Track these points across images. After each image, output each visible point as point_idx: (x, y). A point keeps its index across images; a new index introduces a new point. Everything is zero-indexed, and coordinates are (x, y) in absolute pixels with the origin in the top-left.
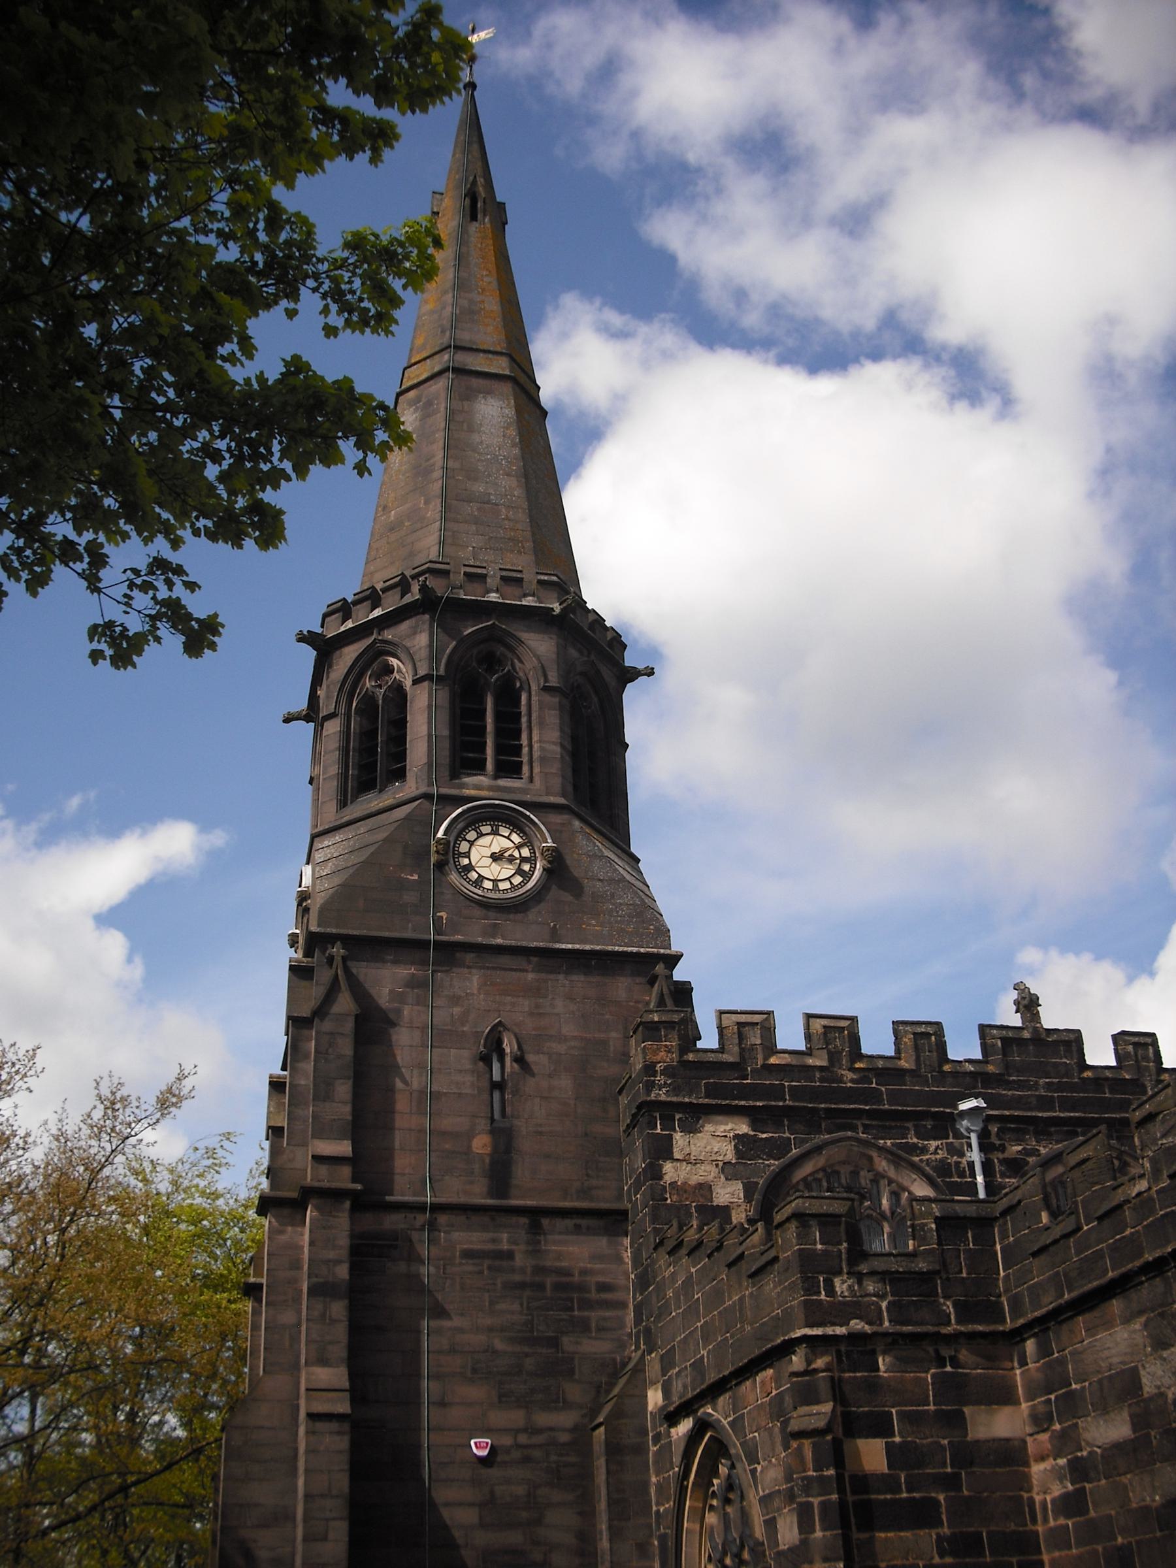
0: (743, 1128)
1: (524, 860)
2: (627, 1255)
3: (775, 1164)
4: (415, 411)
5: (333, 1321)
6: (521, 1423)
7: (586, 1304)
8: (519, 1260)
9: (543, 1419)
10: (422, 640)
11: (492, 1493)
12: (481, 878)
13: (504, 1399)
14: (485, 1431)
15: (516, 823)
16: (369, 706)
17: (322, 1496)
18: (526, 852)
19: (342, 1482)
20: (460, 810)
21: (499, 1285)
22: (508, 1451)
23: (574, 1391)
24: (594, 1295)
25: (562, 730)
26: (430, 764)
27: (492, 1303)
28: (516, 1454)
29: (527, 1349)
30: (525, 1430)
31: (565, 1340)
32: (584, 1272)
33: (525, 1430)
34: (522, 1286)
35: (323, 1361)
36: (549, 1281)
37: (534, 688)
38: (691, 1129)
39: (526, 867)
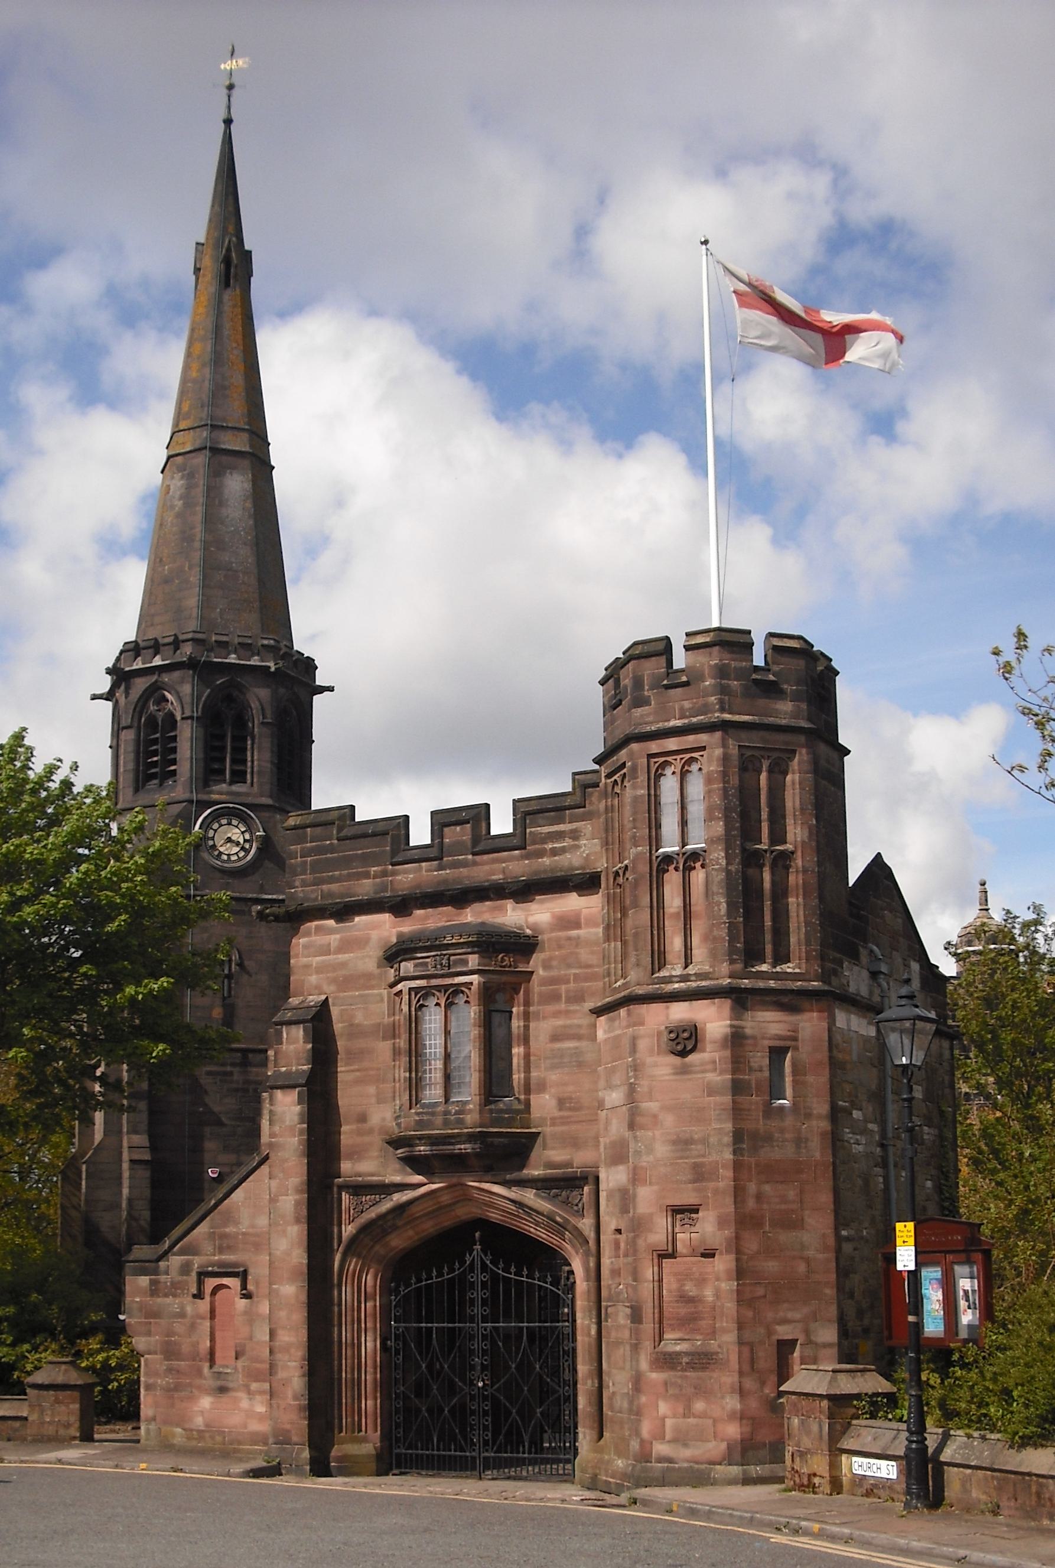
1: (245, 841)
4: (182, 478)
8: (235, 1077)
10: (187, 689)
12: (221, 853)
15: (244, 819)
18: (247, 836)
19: (147, 1193)
20: (209, 811)
25: (272, 752)
26: (191, 777)
34: (237, 1090)
37: (256, 722)
39: (247, 846)
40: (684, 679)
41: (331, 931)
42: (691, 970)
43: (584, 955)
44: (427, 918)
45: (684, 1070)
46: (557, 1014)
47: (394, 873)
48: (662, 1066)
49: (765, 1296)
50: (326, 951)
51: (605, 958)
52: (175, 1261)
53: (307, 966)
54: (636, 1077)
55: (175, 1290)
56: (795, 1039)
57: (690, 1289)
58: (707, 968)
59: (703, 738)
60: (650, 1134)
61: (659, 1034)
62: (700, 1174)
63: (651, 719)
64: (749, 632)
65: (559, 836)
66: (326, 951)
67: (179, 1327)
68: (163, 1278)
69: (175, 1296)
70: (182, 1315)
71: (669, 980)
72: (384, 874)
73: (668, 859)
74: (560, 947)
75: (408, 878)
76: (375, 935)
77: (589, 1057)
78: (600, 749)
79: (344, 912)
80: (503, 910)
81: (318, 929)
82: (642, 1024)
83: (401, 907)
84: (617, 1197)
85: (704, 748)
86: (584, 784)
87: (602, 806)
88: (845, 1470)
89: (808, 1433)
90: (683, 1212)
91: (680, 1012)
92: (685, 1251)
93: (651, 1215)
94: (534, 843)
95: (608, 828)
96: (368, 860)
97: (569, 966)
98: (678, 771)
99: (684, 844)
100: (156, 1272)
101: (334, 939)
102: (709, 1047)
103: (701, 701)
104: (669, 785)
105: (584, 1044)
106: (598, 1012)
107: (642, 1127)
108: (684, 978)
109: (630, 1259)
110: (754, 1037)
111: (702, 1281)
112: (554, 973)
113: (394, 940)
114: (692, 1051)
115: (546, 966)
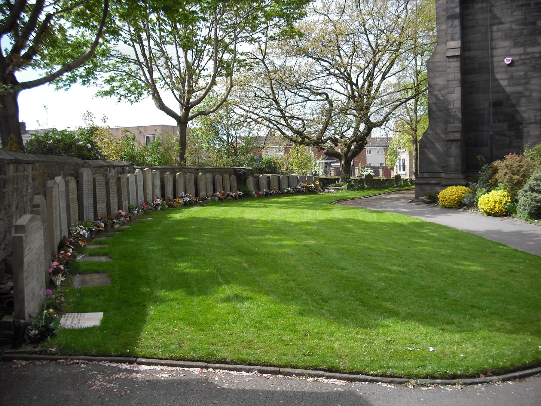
5: (455, 27)
6: (522, 52)
9: (530, 50)
11: (512, 75)
13: (516, 45)
14: (510, 56)
17: (452, 80)
19: (458, 76)
21: (514, 6)
22: (518, 61)
27: (512, 13)
28: (520, 62)
29: (524, 27)
30: (523, 54)
31: (538, 22)
33: (523, 54)
35: (453, 39)
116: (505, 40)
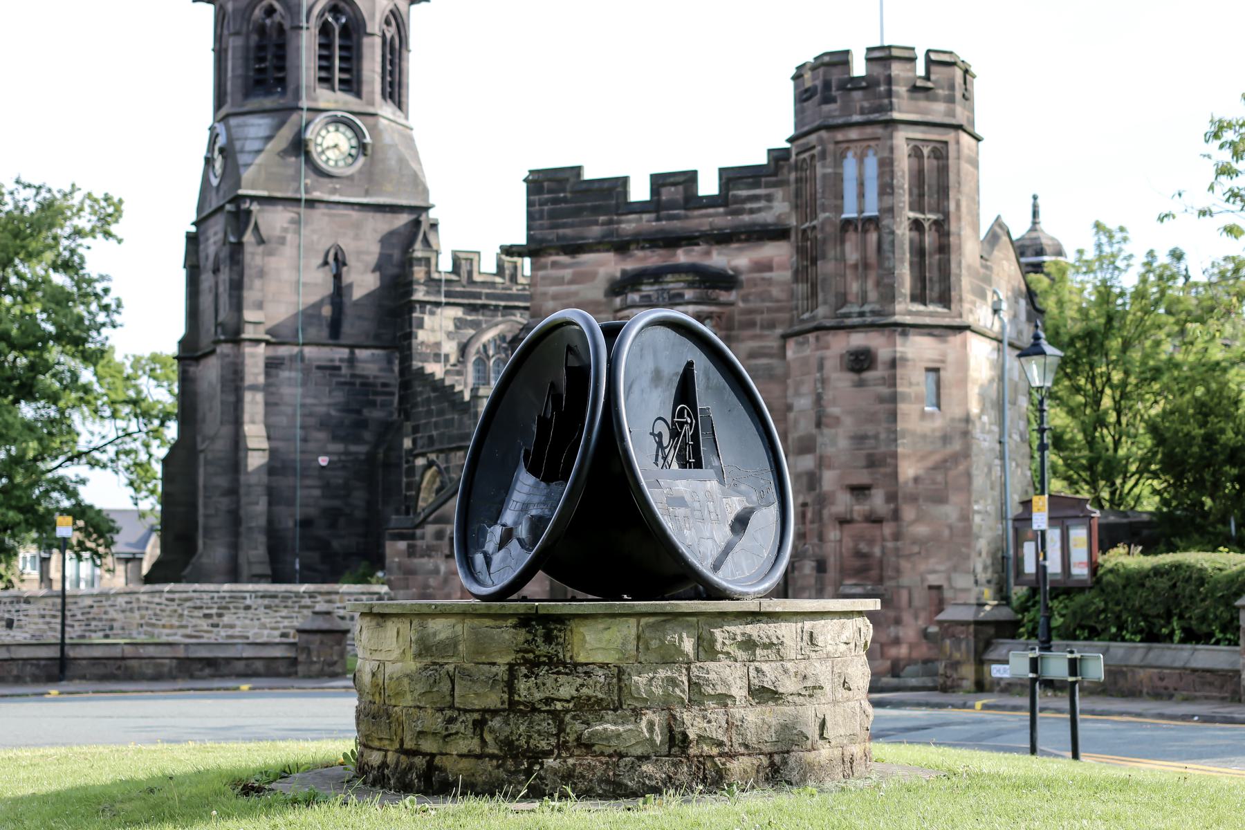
0: (458, 312)
2: (396, 369)
3: (472, 332)
7: (377, 393)
8: (344, 371)
13: (335, 438)
14: (326, 454)
16: (261, 30)
23: (367, 435)
24: (379, 389)
27: (330, 392)
32: (375, 377)
36: (358, 381)
38: (432, 313)
40: (864, 84)
41: (564, 266)
42: (867, 308)
43: (775, 292)
44: (645, 258)
45: (861, 384)
46: (754, 337)
47: (619, 222)
48: (841, 381)
49: (919, 553)
50: (560, 281)
51: (792, 295)
52: (430, 529)
53: (545, 294)
54: (823, 388)
55: (429, 552)
56: (943, 362)
57: (863, 547)
58: (877, 307)
59: (879, 131)
60: (833, 431)
61: (842, 356)
62: (872, 462)
63: (837, 113)
64: (913, 49)
65: (756, 198)
66: (560, 281)
67: (432, 582)
68: (419, 543)
69: (430, 556)
70: (436, 571)
71: (848, 315)
72: (610, 222)
73: (848, 222)
74: (755, 285)
75: (629, 225)
76: (602, 271)
77: (779, 371)
78: (791, 132)
79: (574, 249)
80: (708, 253)
81: (555, 265)
82: (827, 348)
83: (622, 247)
84: (805, 480)
85: (878, 139)
86: (778, 156)
87: (793, 176)
88: (986, 675)
89: (959, 649)
90: (860, 491)
91: (858, 340)
92: (859, 519)
93: (833, 493)
94: (735, 203)
95: (798, 194)
96: (596, 210)
97: (763, 300)
98: (859, 152)
99: (861, 211)
100: (412, 537)
101: (567, 273)
102: (880, 366)
103: (877, 102)
104: (850, 167)
105: (774, 362)
106: (785, 337)
107: (827, 426)
108: (862, 314)
109: (815, 526)
110: (914, 360)
111: (871, 542)
112: (751, 305)
113: (618, 275)
114: (869, 368)
115: (745, 299)
116: (319, 430)
